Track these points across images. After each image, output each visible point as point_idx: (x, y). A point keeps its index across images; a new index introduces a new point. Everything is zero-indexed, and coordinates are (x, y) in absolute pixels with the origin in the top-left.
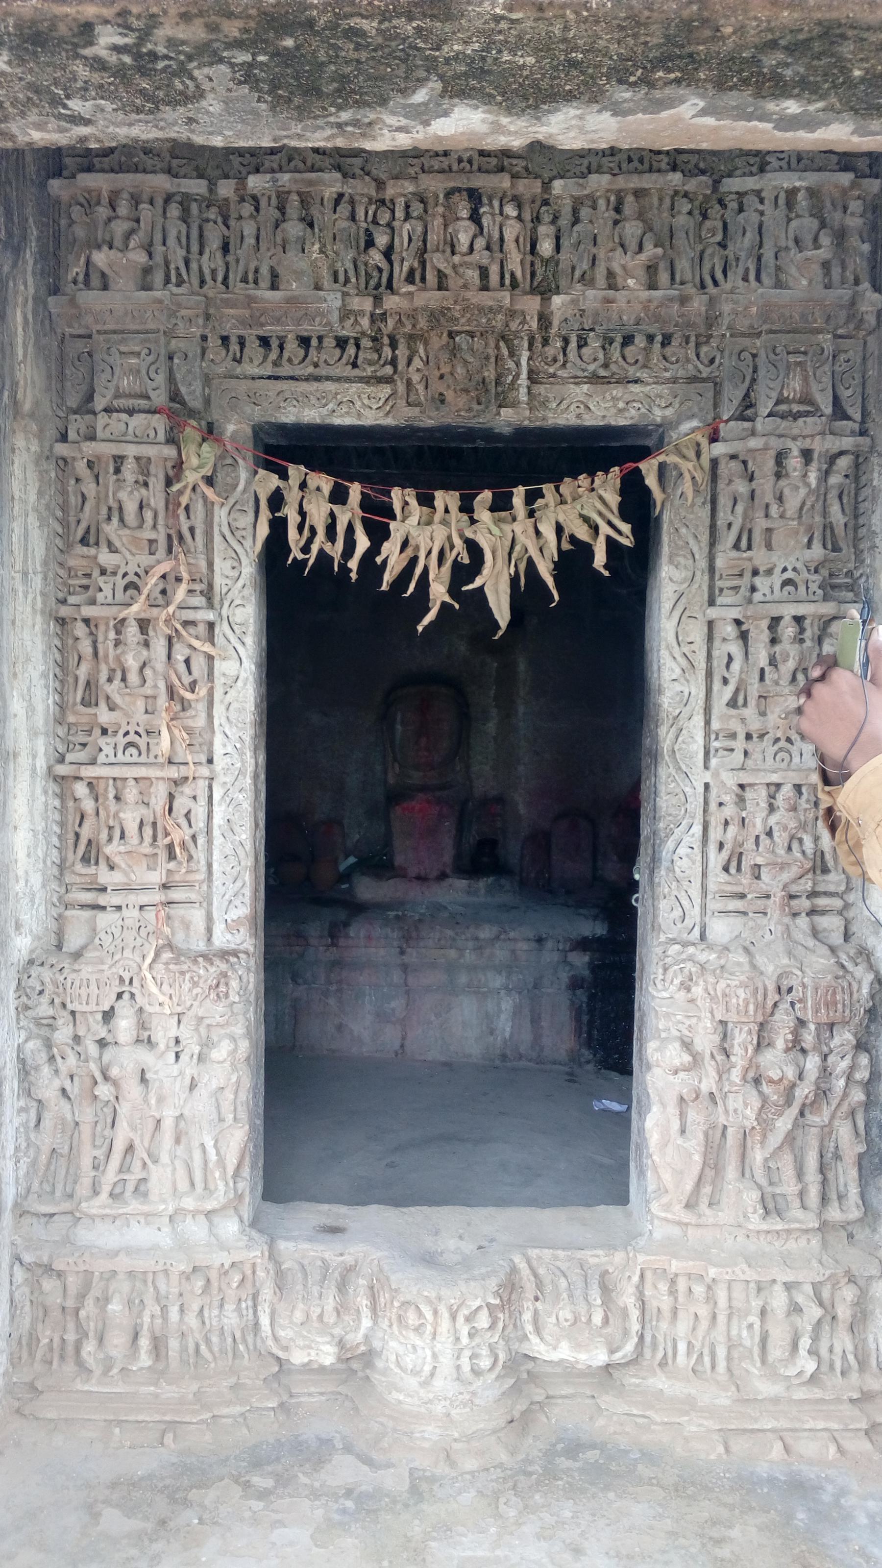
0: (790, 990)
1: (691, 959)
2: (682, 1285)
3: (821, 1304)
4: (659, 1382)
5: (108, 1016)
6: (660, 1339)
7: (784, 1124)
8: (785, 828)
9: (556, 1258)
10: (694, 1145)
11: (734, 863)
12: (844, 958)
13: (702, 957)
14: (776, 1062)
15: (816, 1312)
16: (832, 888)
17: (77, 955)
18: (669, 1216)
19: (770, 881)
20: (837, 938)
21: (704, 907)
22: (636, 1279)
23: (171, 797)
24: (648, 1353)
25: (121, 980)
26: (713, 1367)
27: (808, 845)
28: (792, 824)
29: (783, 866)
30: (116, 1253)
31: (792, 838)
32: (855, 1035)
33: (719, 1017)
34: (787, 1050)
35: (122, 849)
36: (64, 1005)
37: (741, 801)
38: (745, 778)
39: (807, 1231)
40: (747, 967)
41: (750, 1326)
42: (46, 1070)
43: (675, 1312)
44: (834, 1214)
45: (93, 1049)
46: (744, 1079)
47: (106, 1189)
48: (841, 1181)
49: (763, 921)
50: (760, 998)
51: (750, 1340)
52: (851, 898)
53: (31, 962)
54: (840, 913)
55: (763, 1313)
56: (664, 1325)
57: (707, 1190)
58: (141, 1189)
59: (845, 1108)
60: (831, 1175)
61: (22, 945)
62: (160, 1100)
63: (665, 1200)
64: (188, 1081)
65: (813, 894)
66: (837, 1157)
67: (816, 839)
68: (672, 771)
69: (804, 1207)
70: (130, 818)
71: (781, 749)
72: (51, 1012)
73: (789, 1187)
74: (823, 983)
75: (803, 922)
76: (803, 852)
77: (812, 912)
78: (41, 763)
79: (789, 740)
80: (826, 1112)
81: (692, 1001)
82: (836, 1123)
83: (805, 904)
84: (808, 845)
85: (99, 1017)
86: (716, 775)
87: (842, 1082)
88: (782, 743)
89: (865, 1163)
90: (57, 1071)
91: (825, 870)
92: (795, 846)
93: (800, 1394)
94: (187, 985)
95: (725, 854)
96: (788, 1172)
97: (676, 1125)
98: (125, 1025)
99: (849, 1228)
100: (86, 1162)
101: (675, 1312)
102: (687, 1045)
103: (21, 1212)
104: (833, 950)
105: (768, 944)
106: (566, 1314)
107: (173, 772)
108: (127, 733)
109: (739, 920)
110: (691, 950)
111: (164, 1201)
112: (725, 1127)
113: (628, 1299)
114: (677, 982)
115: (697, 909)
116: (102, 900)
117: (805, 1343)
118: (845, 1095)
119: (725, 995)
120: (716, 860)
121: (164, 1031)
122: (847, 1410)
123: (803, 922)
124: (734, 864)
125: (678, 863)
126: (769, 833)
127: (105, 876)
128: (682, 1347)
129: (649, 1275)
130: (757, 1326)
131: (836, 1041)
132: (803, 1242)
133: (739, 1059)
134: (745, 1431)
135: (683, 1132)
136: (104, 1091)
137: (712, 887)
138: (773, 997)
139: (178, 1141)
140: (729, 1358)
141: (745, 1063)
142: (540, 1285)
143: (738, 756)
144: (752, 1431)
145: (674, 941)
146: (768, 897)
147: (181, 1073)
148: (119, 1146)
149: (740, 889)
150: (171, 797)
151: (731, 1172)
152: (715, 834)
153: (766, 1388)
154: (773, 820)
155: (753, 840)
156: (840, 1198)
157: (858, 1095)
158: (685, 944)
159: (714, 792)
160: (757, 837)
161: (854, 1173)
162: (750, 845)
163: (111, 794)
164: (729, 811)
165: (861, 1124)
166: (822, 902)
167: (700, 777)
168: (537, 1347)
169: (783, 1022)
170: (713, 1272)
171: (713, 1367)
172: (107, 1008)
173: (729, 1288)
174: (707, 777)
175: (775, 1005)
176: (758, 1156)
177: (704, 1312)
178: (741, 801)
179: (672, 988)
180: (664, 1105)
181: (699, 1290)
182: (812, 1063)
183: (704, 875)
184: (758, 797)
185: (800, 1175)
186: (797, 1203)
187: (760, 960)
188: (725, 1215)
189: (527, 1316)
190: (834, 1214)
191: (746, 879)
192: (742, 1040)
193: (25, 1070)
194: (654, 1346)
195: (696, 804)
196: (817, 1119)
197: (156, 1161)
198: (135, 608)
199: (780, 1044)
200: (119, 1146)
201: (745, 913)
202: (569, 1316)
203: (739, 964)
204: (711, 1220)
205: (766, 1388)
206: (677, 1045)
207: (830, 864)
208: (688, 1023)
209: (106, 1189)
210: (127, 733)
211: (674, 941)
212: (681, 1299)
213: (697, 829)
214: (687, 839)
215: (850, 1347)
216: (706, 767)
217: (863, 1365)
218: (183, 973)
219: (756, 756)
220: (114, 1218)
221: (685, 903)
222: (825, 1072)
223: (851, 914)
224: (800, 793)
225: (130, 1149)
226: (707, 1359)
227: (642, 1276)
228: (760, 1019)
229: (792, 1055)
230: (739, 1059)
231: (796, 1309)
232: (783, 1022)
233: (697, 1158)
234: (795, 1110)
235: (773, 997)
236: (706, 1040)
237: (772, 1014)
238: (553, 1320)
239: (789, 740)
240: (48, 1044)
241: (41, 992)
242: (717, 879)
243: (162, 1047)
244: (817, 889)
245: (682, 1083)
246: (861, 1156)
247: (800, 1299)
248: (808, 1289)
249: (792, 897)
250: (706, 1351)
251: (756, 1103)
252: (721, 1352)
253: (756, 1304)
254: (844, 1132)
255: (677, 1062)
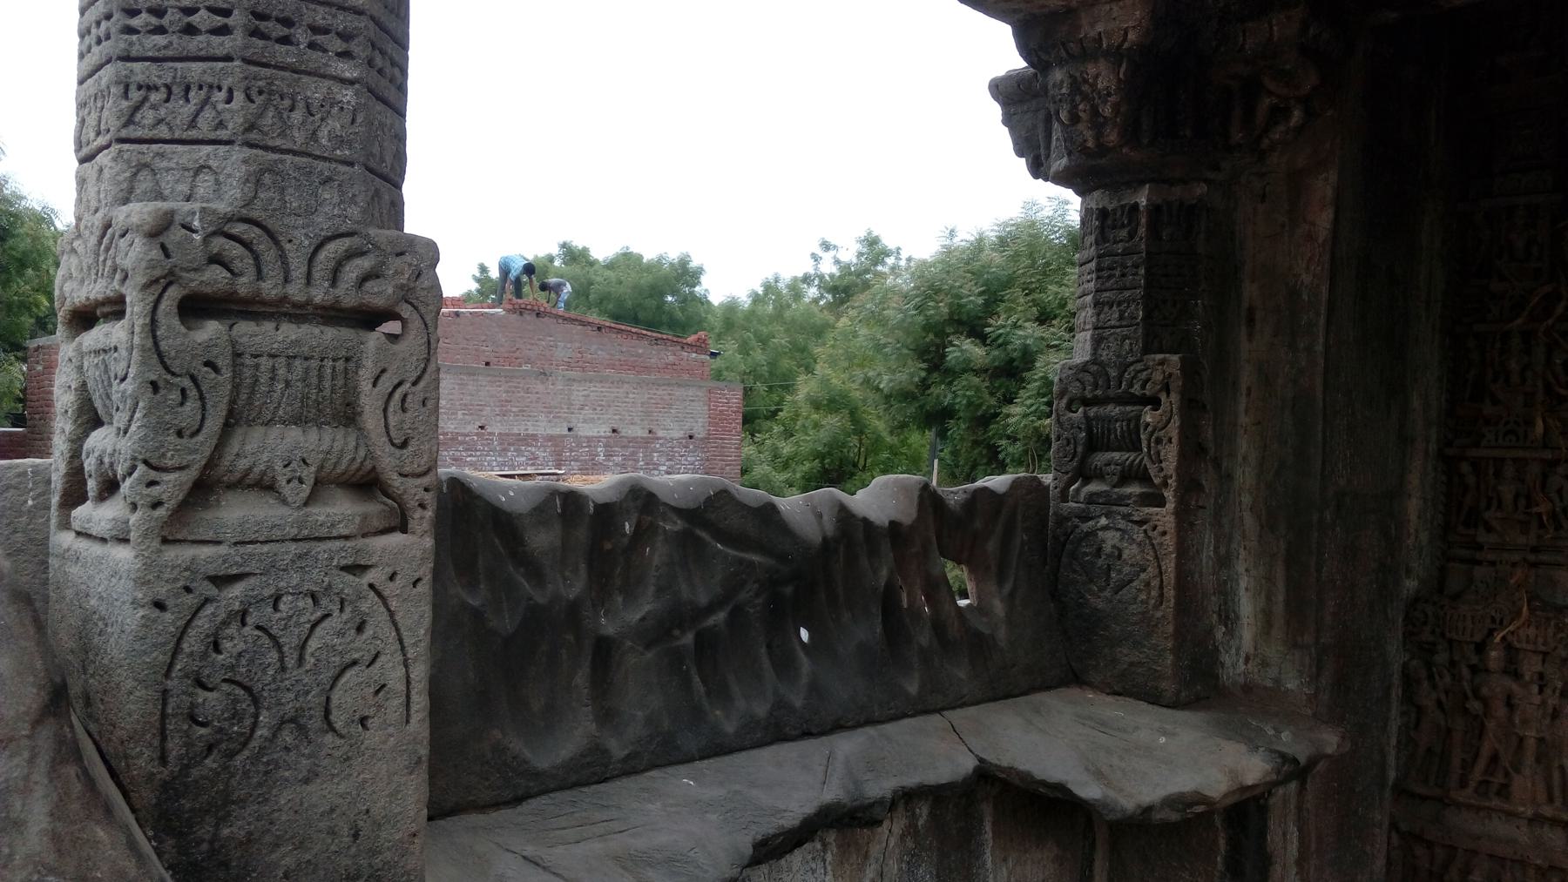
5: (1481, 648)
17: (1456, 597)
23: (1545, 476)
25: (1493, 620)
30: (1479, 838)
35: (1499, 515)
36: (1443, 635)
42: (1425, 684)
45: (1465, 672)
47: (1472, 784)
53: (1416, 600)
58: (1504, 791)
61: (1410, 585)
62: (1525, 722)
64: (1550, 711)
70: (1507, 491)
72: (1431, 639)
78: (1433, 447)
85: (1472, 647)
90: (1434, 687)
94: (1551, 631)
98: (1495, 655)
100: (1456, 762)
103: (1400, 791)
107: (1548, 455)
108: (1507, 423)
111: (1524, 805)
116: (1478, 556)
121: (1531, 666)
127: (1482, 537)
136: (1475, 706)
139: (1538, 761)
147: (1544, 703)
148: (1485, 752)
150: (1545, 476)
163: (1491, 471)
172: (1478, 638)
193: (1408, 681)
197: (1518, 771)
198: (1519, 321)
200: (1485, 752)
209: (1472, 784)
210: (1507, 423)
218: (1548, 619)
220: (1479, 809)
225: (1495, 759)
240: (1429, 665)
241: (1425, 623)
243: (1527, 678)
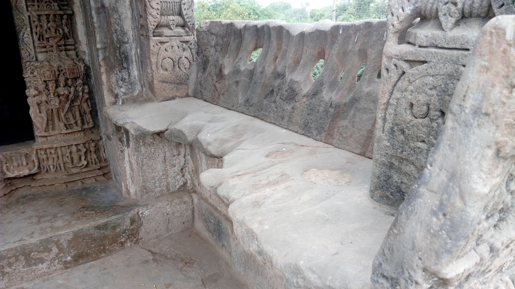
0: (62, 70)
1: (33, 65)
2: (48, 151)
3: (86, 148)
4: (47, 176)
6: (45, 166)
7: (67, 106)
8: (53, 27)
9: (12, 153)
10: (44, 115)
11: (41, 37)
12: (75, 61)
13: (36, 64)
14: (62, 90)
15: (84, 150)
16: (70, 43)
18: (41, 135)
19: (52, 42)
20: (74, 57)
21: (35, 52)
22: (35, 152)
24: (42, 170)
26: (61, 169)
27: (61, 31)
28: (55, 26)
29: (55, 38)
31: (56, 30)
32: (82, 81)
33: (43, 80)
34: (64, 87)
37: (39, 20)
38: (39, 13)
39: (79, 131)
40: (48, 65)
41: (68, 157)
43: (48, 158)
44: (86, 126)
46: (54, 95)
48: (88, 119)
49: (51, 53)
50: (53, 73)
51: (69, 161)
52: (77, 46)
54: (75, 49)
55: (71, 153)
56: (45, 162)
57: (51, 127)
59: (84, 100)
60: (84, 118)
63: (39, 131)
65: (65, 45)
66: (86, 113)
67: (63, 30)
68: (17, 12)
69: (77, 125)
71: (48, 5)
73: (73, 122)
74: (70, 68)
75: (63, 53)
76: (60, 34)
77: (66, 50)
79: (50, 2)
80: (79, 101)
81: (34, 76)
82: (82, 104)
83: (63, 48)
84: (61, 31)
86: (31, 13)
87: (81, 93)
88: (48, 3)
89: (93, 113)
91: (68, 39)
92: (57, 32)
93: (85, 170)
95: (38, 36)
96: (71, 118)
97: (38, 111)
99: (92, 130)
101: (48, 158)
102: (36, 89)
104: (72, 59)
105: (54, 59)
106: (15, 164)
109: (46, 54)
110: (32, 63)
112: (52, 110)
113: (34, 157)
114: (29, 72)
115: (33, 52)
117: (83, 158)
118: (83, 97)
119: (43, 74)
120: (36, 38)
122: (97, 171)
123: (63, 53)
124: (41, 38)
125: (25, 39)
126: (49, 29)
128: (51, 167)
129: (39, 151)
130: (69, 156)
131: (78, 83)
132: (79, 135)
133: (52, 91)
134: (71, 181)
135: (40, 112)
137: (36, 45)
138: (57, 73)
140: (64, 167)
141: (54, 91)
142: (8, 160)
143: (36, 7)
144: (73, 181)
145: (28, 61)
146: (52, 47)
149: (43, 45)
151: (56, 121)
152: (34, 30)
153: (75, 171)
154: (49, 25)
155: (45, 31)
156: (88, 123)
157: (86, 96)
158: (31, 62)
159: (31, 18)
160: (46, 30)
161: (89, 116)
162: (44, 32)
164: (37, 23)
165: (90, 104)
166: (68, 47)
167: (27, 14)
168: (10, 175)
169: (62, 79)
170: (55, 146)
171: (61, 169)
173: (61, 149)
174: (28, 14)
175: (59, 75)
176: (62, 115)
177: (55, 156)
178: (39, 20)
179: (29, 74)
180: (34, 107)
181: (53, 151)
182: (72, 89)
183: (33, 42)
184: (44, 18)
185: (75, 118)
186: (75, 125)
187: (52, 63)
188: (57, 132)
189: (4, 168)
190: (86, 126)
191: (45, 42)
192: (51, 85)
194: (44, 168)
195: (27, 22)
196: (77, 104)
199: (62, 85)
201: (47, 52)
202: (16, 164)
203: (46, 65)
204: (53, 134)
205: (75, 171)
206: (33, 89)
207: (69, 36)
208: (35, 82)
211: (28, 61)
212: (49, 155)
213: (29, 29)
214: (26, 32)
215: (96, 157)
216: (28, 10)
217: (100, 161)
219: (41, 6)
221: (29, 51)
222: (76, 91)
223: (77, 50)
224: (56, 17)
226: (59, 168)
227: (37, 152)
228: (54, 79)
229: (66, 87)
230: (52, 91)
231: (79, 150)
232: (62, 79)
233: (45, 118)
234: (69, 102)
235: (57, 73)
236: (42, 87)
237: (58, 77)
238: (12, 167)
239: (50, 2)
242: (37, 43)
244: (66, 44)
245: (37, 99)
246: (90, 111)
247: (80, 148)
248: (82, 145)
249: (59, 46)
250: (58, 166)
251: (58, 101)
252: (62, 165)
253: (68, 151)
254: (85, 106)
255: (34, 94)
